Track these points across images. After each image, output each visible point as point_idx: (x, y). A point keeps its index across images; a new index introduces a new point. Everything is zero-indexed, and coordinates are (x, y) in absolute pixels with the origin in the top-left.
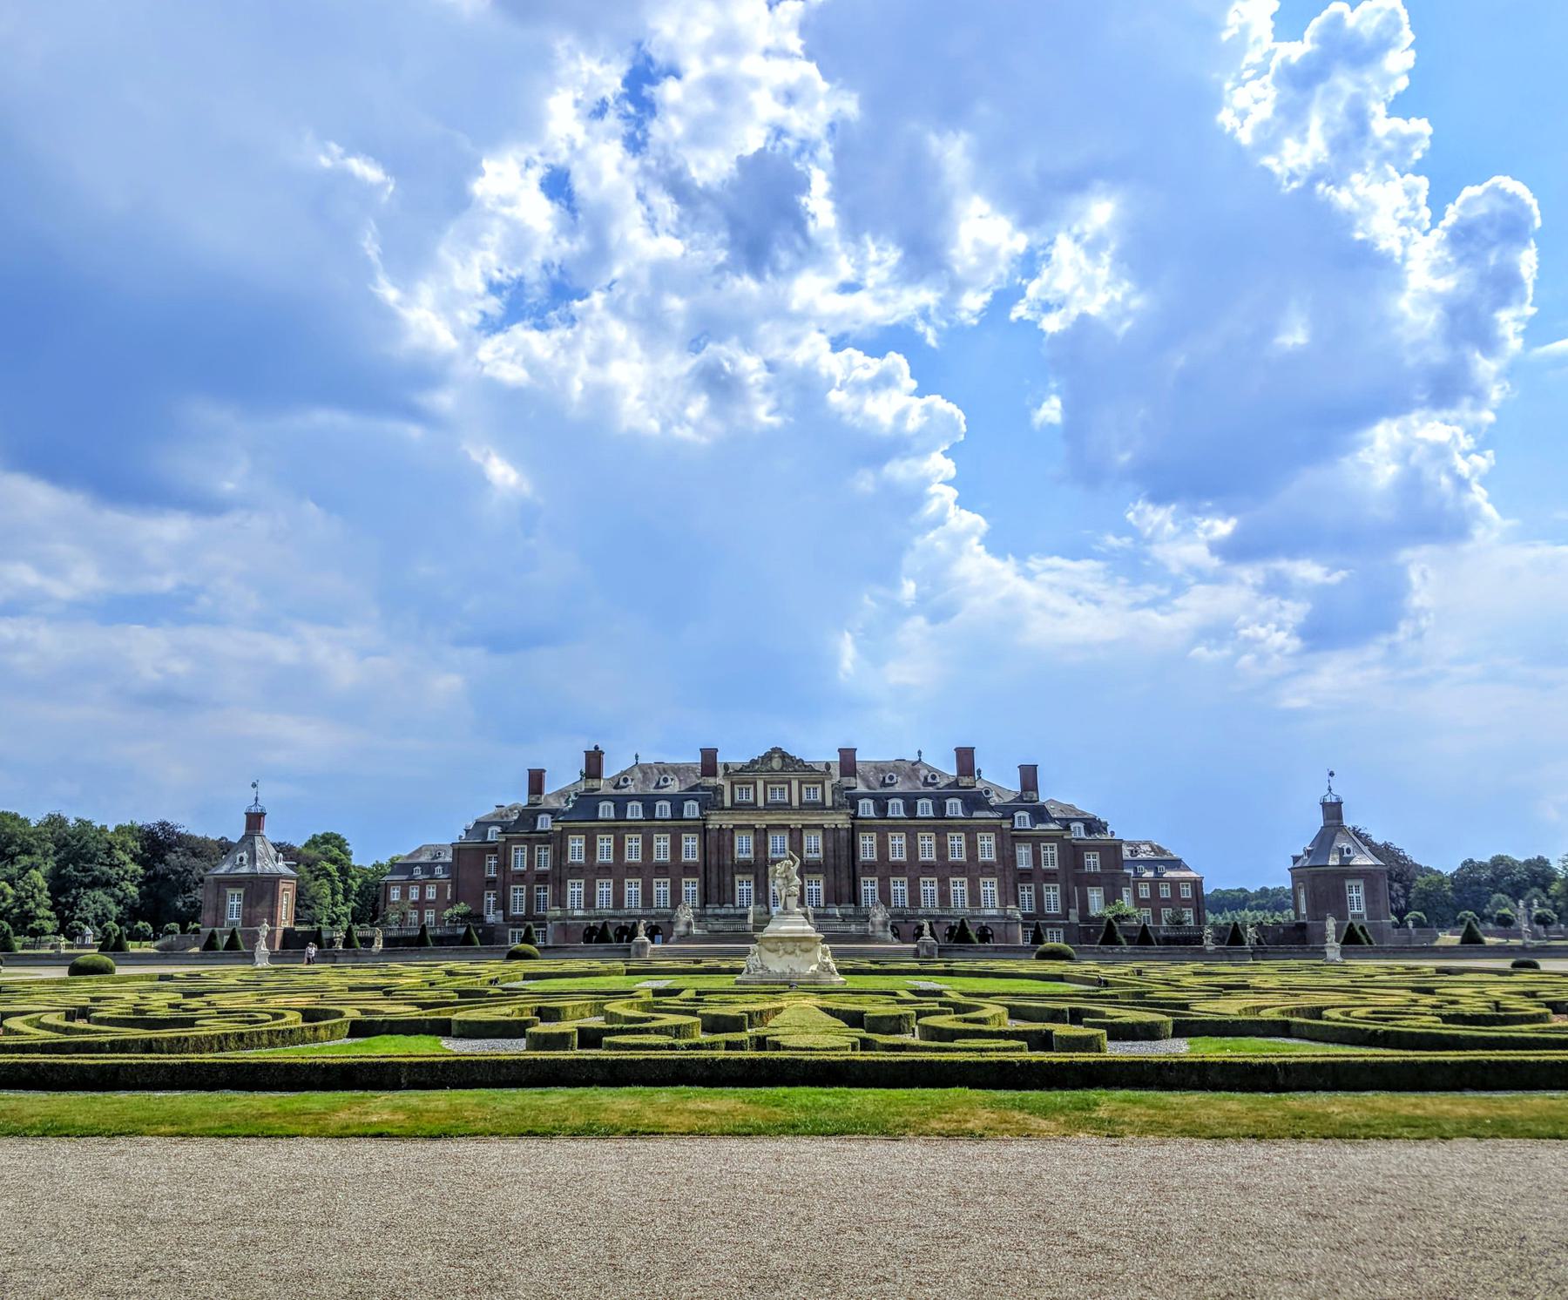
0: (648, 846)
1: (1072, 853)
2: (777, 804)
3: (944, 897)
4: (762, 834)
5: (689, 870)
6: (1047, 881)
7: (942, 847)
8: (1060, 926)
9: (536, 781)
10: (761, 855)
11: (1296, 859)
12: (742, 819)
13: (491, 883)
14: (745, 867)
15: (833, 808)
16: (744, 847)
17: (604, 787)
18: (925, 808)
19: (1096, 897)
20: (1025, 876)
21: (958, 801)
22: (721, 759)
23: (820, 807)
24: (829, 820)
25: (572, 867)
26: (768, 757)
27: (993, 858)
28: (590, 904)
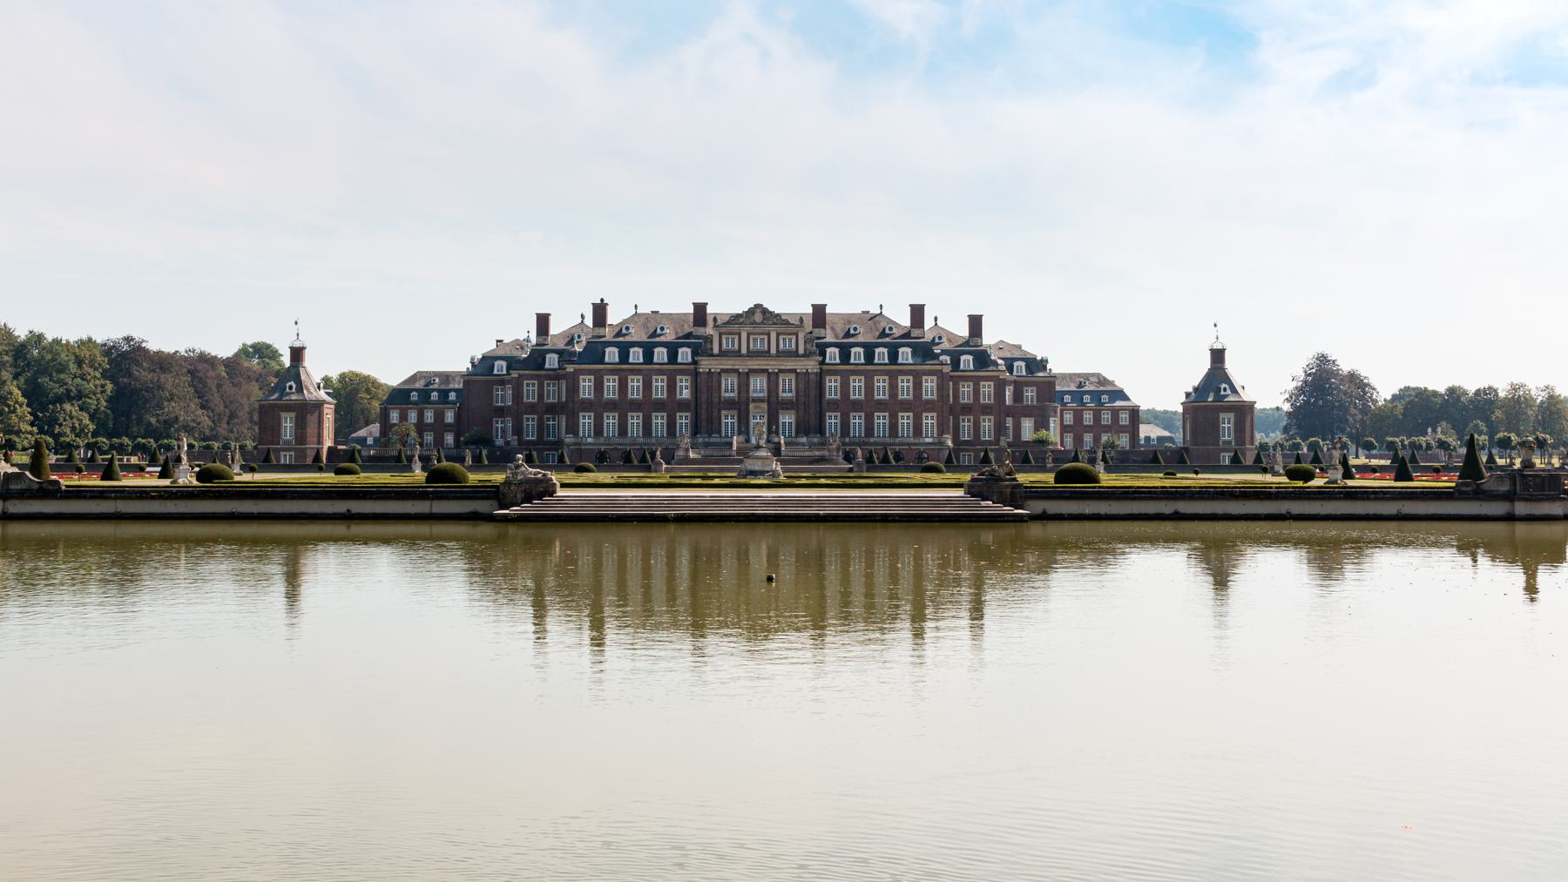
0: (647, 386)
4: (744, 378)
5: (683, 406)
6: (984, 413)
7: (893, 387)
9: (543, 321)
11: (1188, 395)
12: (728, 364)
13: (501, 412)
14: (730, 404)
15: (804, 356)
16: (729, 387)
17: (608, 334)
18: (881, 354)
19: (1027, 425)
20: (967, 409)
22: (709, 310)
23: (795, 354)
25: (584, 401)
26: (751, 312)
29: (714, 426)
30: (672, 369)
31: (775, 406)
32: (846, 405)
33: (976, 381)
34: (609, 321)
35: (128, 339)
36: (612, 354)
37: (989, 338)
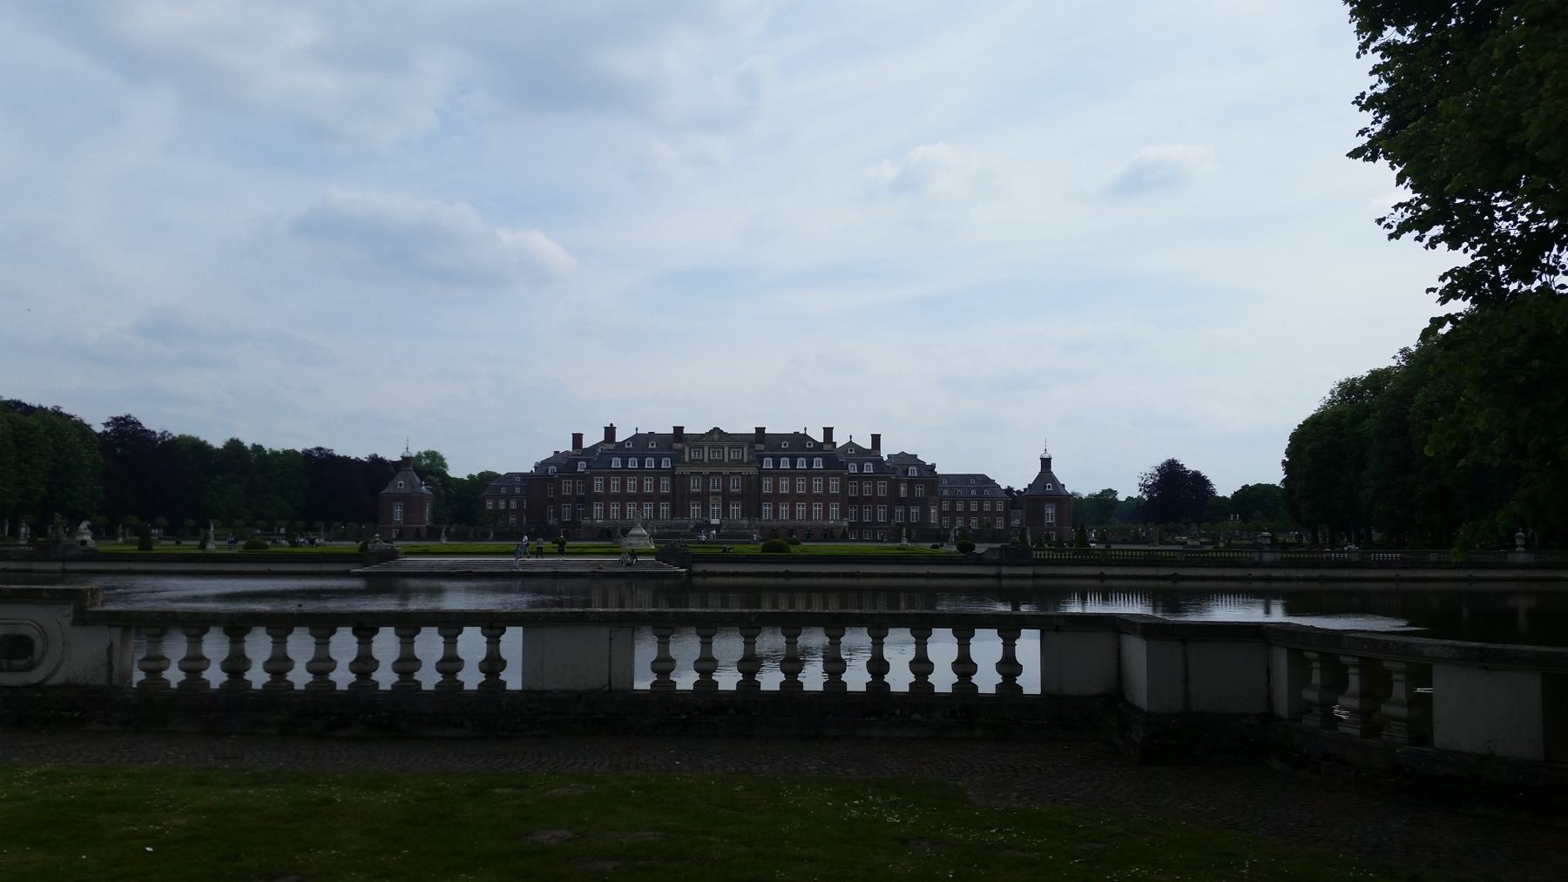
3: (809, 513)
5: (664, 498)
7: (809, 485)
9: (577, 438)
14: (696, 496)
16: (695, 486)
20: (868, 500)
24: (744, 471)
29: (685, 512)
31: (727, 498)
32: (776, 498)
35: (319, 449)
37: (885, 452)
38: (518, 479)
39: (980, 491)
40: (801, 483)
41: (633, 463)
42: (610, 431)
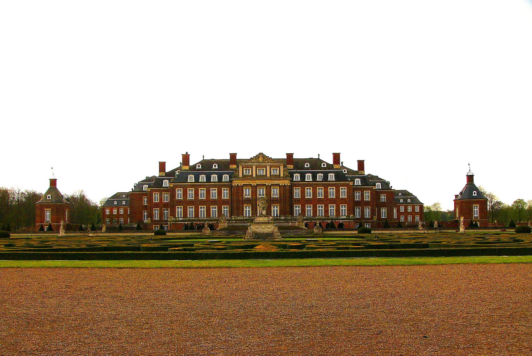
0: (208, 192)
1: (376, 194)
2: (261, 176)
3: (326, 211)
5: (225, 202)
7: (326, 192)
8: (369, 222)
9: (162, 166)
10: (254, 197)
11: (456, 196)
13: (146, 208)
14: (248, 201)
16: (247, 193)
19: (384, 210)
20: (358, 204)
21: (333, 175)
22: (238, 157)
24: (281, 183)
26: (257, 157)
27: (346, 197)
28: (185, 215)
29: (240, 212)
30: (220, 185)
32: (303, 202)
33: (362, 190)
34: (190, 165)
36: (191, 178)
37: (367, 172)
38: (124, 196)
39: (405, 200)
40: (320, 191)
41: (203, 178)
42: (186, 158)
